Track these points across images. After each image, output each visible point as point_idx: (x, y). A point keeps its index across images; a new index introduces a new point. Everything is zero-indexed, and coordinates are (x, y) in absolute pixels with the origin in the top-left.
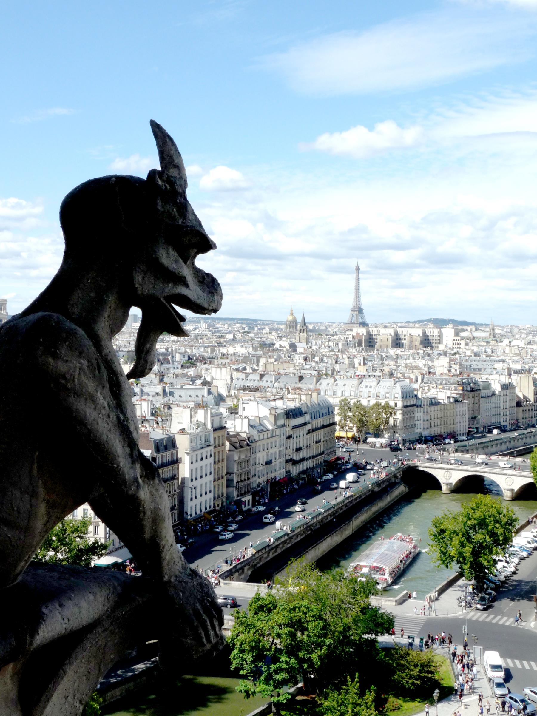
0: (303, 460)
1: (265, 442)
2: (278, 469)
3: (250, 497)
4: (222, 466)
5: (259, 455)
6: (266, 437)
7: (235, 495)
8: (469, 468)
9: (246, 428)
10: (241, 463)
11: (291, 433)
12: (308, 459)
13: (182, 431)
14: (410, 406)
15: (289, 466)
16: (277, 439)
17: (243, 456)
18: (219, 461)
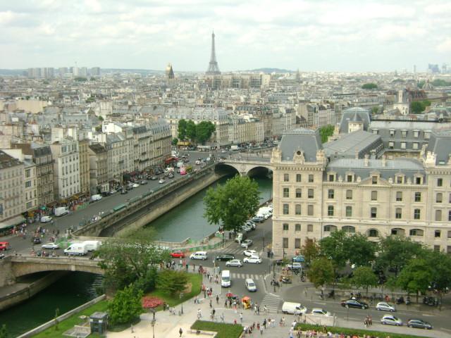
0: (147, 160)
1: (118, 149)
2: (128, 166)
3: (108, 184)
4: (87, 166)
5: (113, 157)
6: (119, 145)
7: (97, 183)
8: (256, 162)
9: (105, 141)
10: (99, 162)
11: (138, 143)
12: (151, 160)
13: (57, 143)
14: (224, 125)
15: (137, 165)
16: (128, 147)
17: (102, 158)
18: (84, 162)
